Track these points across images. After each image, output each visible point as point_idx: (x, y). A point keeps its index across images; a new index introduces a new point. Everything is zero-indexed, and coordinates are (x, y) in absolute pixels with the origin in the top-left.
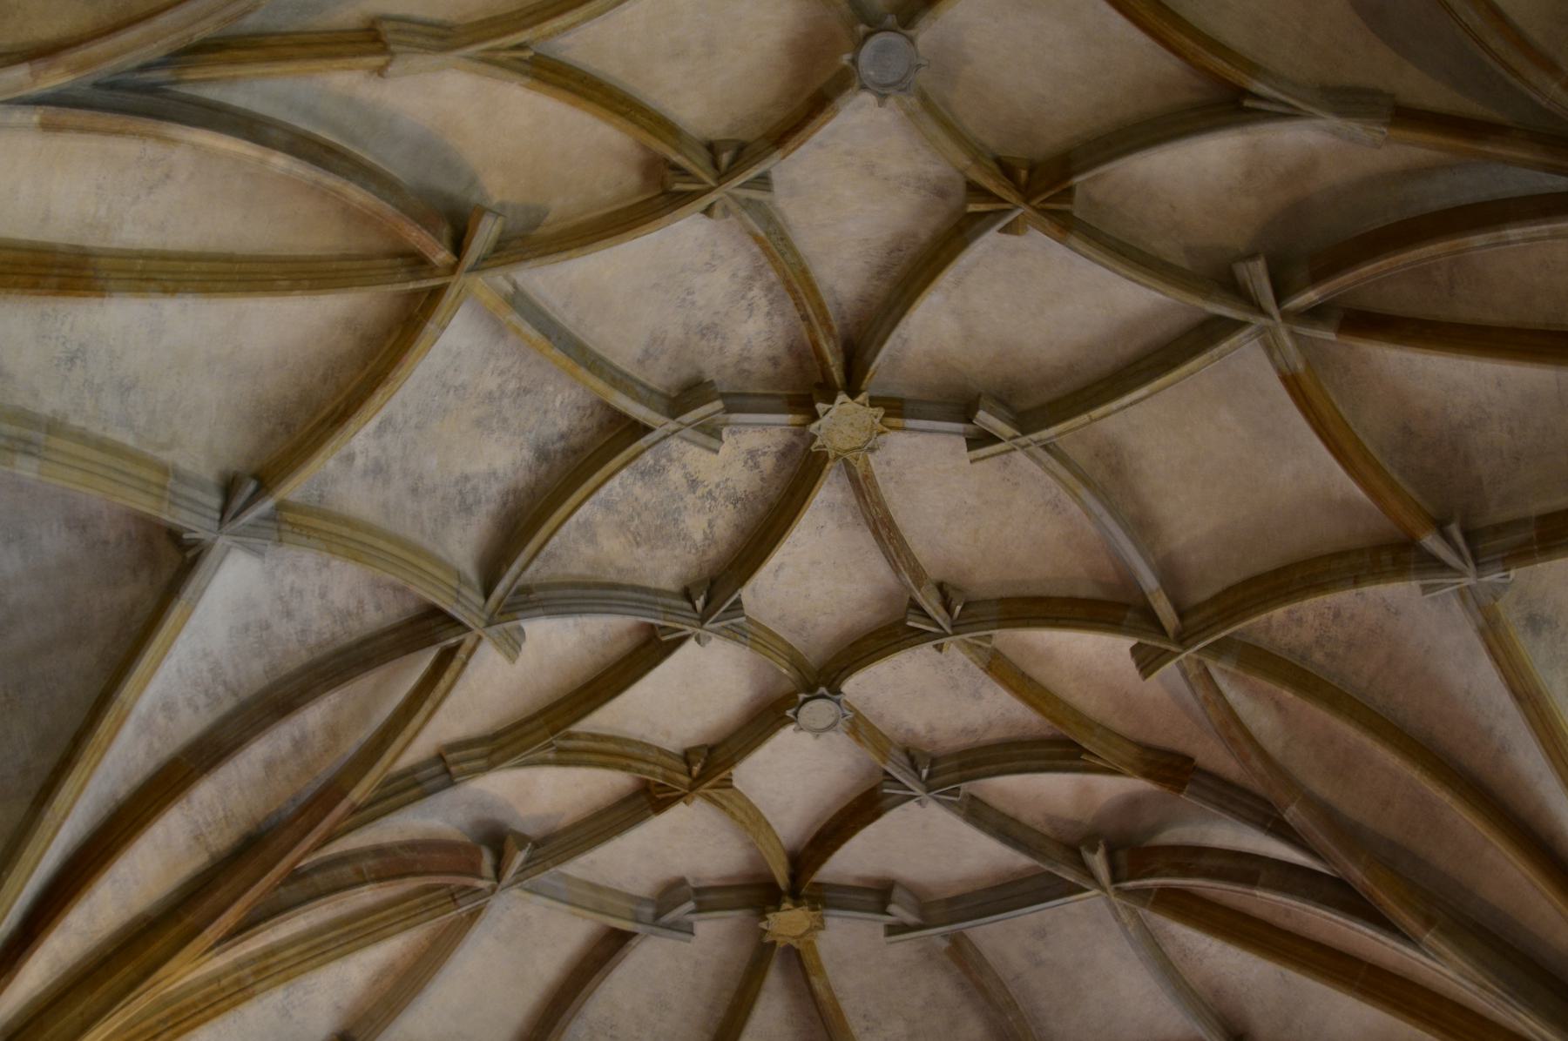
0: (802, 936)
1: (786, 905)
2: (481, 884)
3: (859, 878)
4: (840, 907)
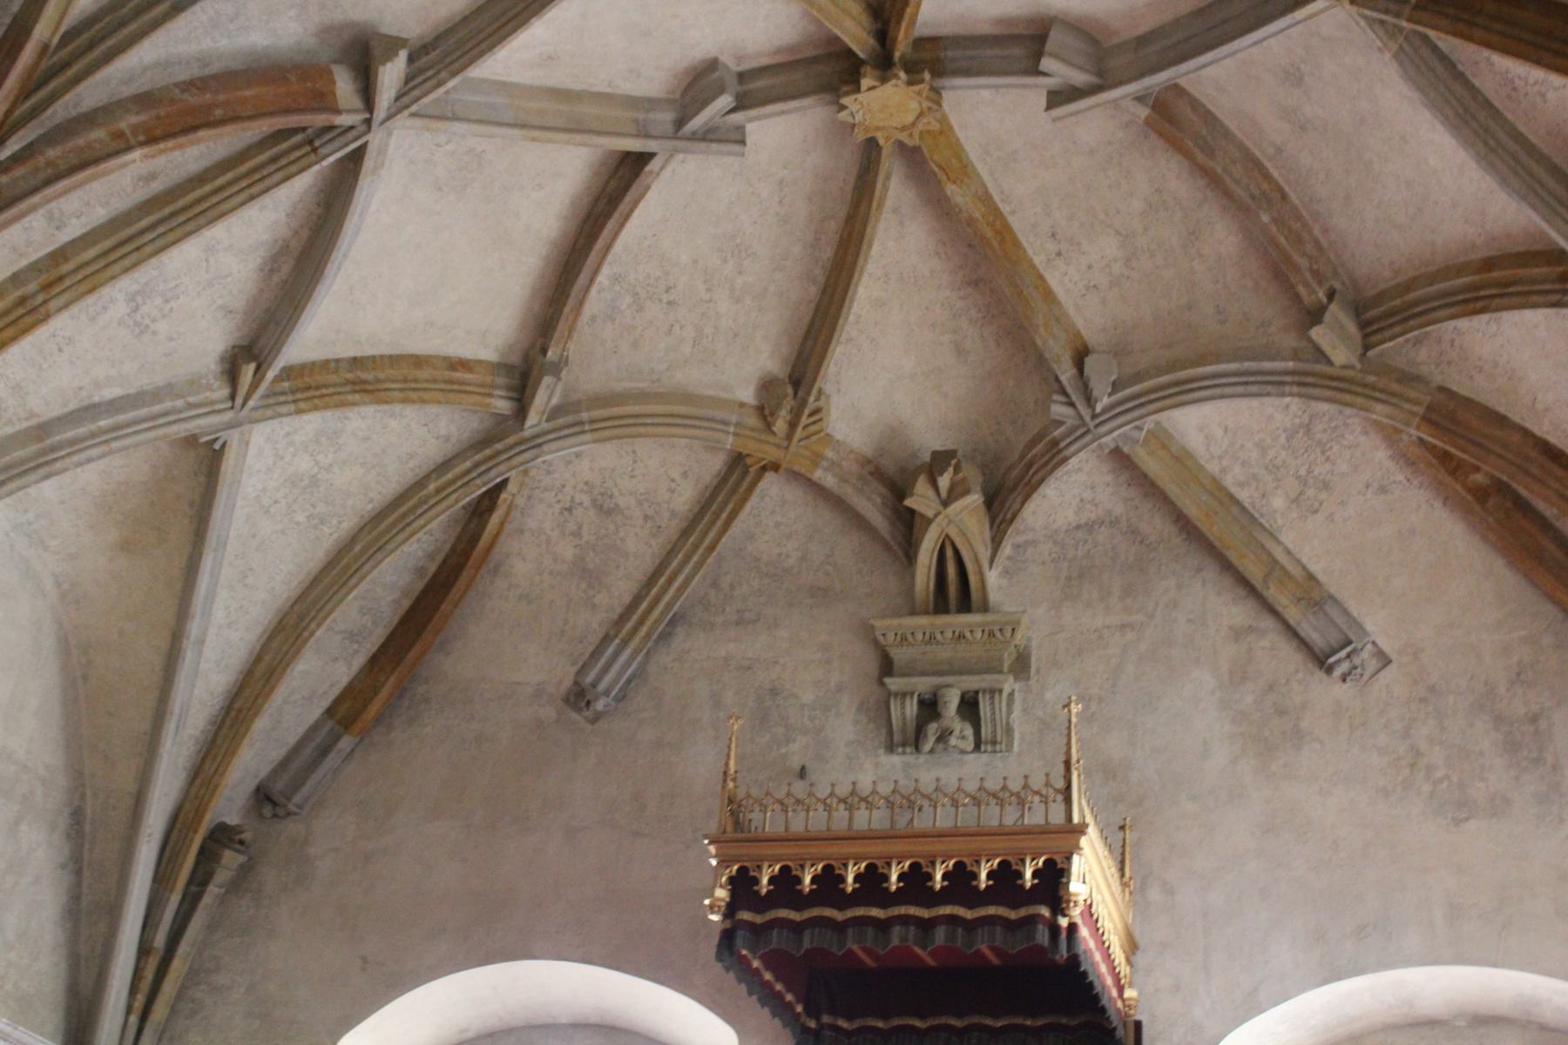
0: (913, 124)
1: (866, 82)
2: (344, 120)
3: (999, 21)
4: (967, 73)
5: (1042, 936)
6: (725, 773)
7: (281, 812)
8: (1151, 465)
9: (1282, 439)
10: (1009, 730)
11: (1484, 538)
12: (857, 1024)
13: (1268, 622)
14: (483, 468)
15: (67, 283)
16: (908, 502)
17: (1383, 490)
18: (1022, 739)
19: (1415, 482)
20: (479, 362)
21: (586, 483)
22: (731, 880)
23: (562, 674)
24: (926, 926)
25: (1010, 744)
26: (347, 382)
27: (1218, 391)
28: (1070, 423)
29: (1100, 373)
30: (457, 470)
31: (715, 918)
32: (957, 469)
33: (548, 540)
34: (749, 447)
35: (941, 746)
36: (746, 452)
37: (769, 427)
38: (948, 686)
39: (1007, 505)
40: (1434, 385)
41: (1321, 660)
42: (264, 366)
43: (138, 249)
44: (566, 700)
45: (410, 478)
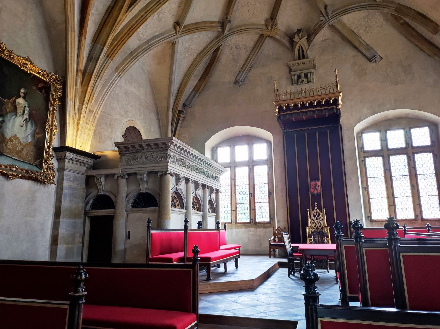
5: (335, 111)
6: (275, 90)
7: (188, 107)
8: (339, 27)
9: (363, 19)
10: (313, 79)
11: (401, 33)
12: (293, 130)
13: (359, 54)
14: (218, 42)
15: (149, 11)
16: (294, 40)
17: (381, 26)
18: (316, 80)
19: (388, 24)
20: (215, 22)
21: (234, 43)
22: (279, 108)
23: (233, 79)
24: (314, 111)
25: (314, 82)
26: (194, 28)
27: (353, 10)
28: (324, 20)
29: (329, 10)
30: (213, 43)
31: (276, 114)
32: (302, 33)
33: (228, 55)
34: (264, 32)
35: (302, 83)
36: (263, 34)
37: (268, 29)
38: (302, 72)
39: (311, 38)
40: (397, 3)
41: (370, 60)
42: (181, 26)
43: (160, 3)
44: (234, 83)
45: (205, 46)
